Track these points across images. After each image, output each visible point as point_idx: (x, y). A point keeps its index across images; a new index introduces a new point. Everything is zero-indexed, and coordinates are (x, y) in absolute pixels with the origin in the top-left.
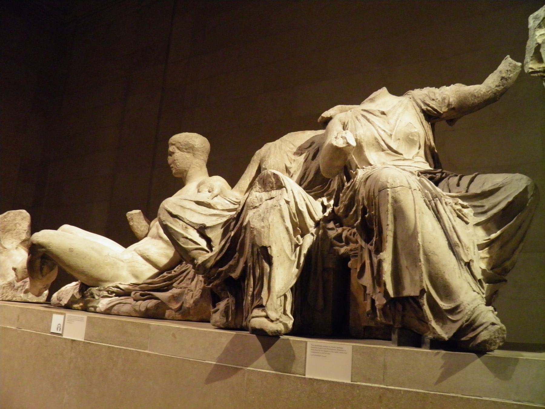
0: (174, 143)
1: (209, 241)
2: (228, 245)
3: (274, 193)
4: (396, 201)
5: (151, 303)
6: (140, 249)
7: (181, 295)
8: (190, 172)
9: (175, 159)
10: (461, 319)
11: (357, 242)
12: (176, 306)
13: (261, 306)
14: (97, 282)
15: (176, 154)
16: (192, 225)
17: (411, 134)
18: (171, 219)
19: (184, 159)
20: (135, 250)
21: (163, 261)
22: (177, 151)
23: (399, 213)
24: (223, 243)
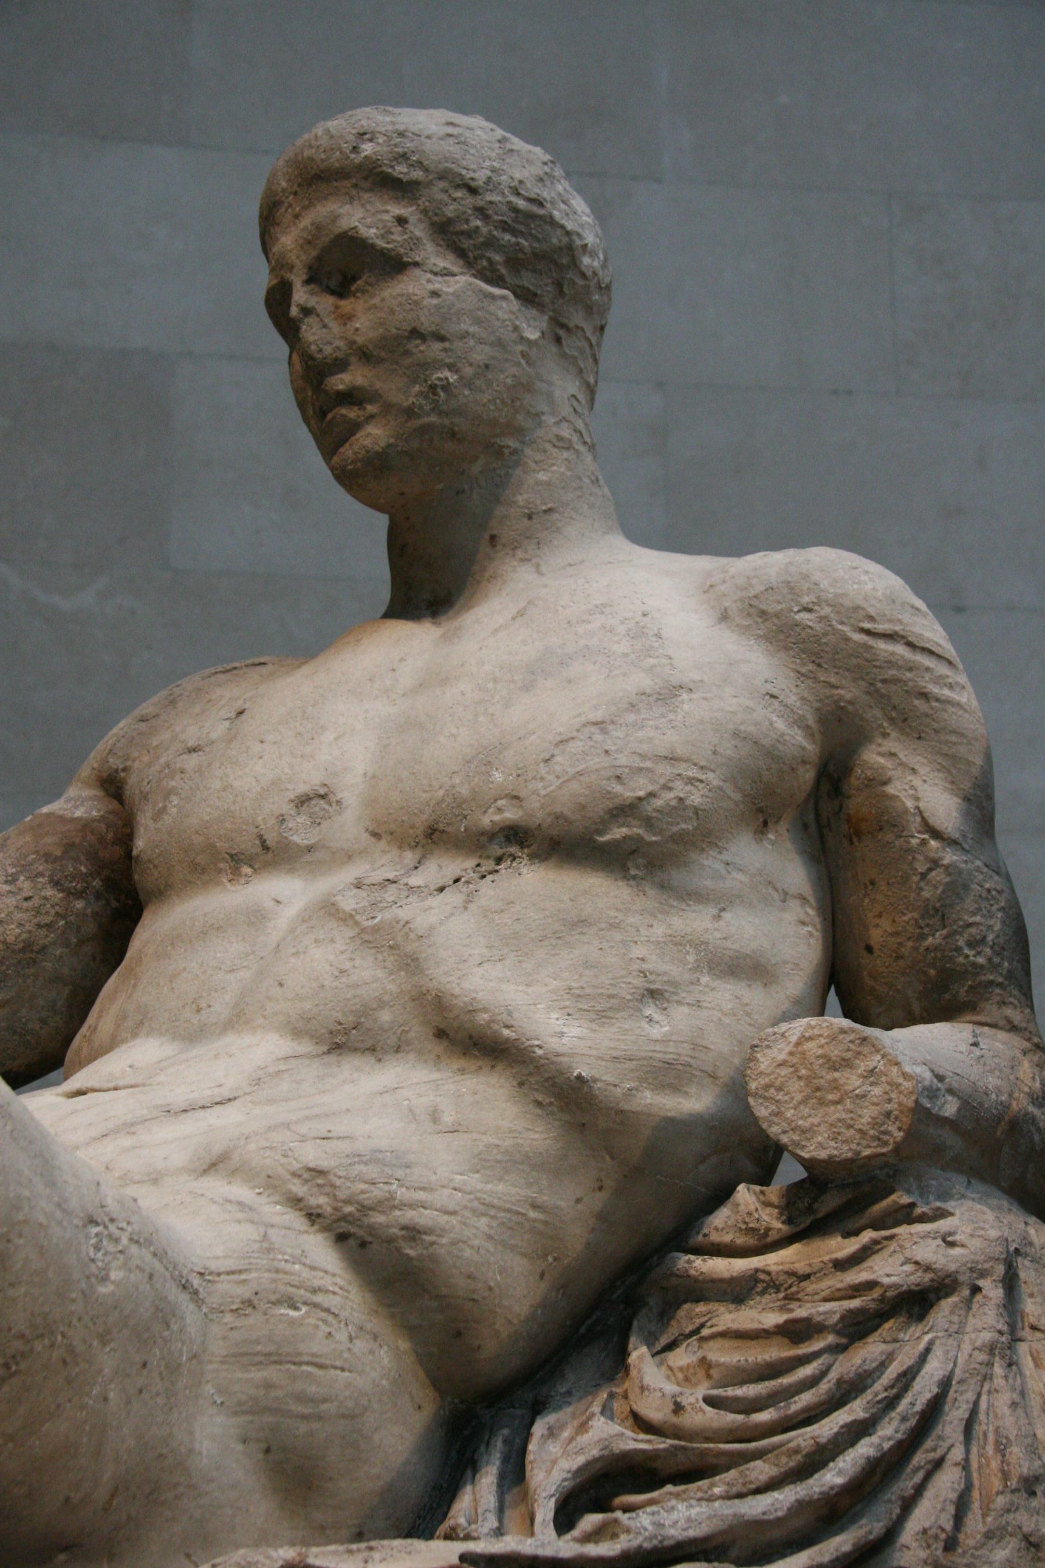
0: (400, 170)
6: (311, 1155)
8: (543, 473)
9: (427, 324)
15: (413, 285)
19: (500, 344)
20: (216, 1164)
22: (434, 255)
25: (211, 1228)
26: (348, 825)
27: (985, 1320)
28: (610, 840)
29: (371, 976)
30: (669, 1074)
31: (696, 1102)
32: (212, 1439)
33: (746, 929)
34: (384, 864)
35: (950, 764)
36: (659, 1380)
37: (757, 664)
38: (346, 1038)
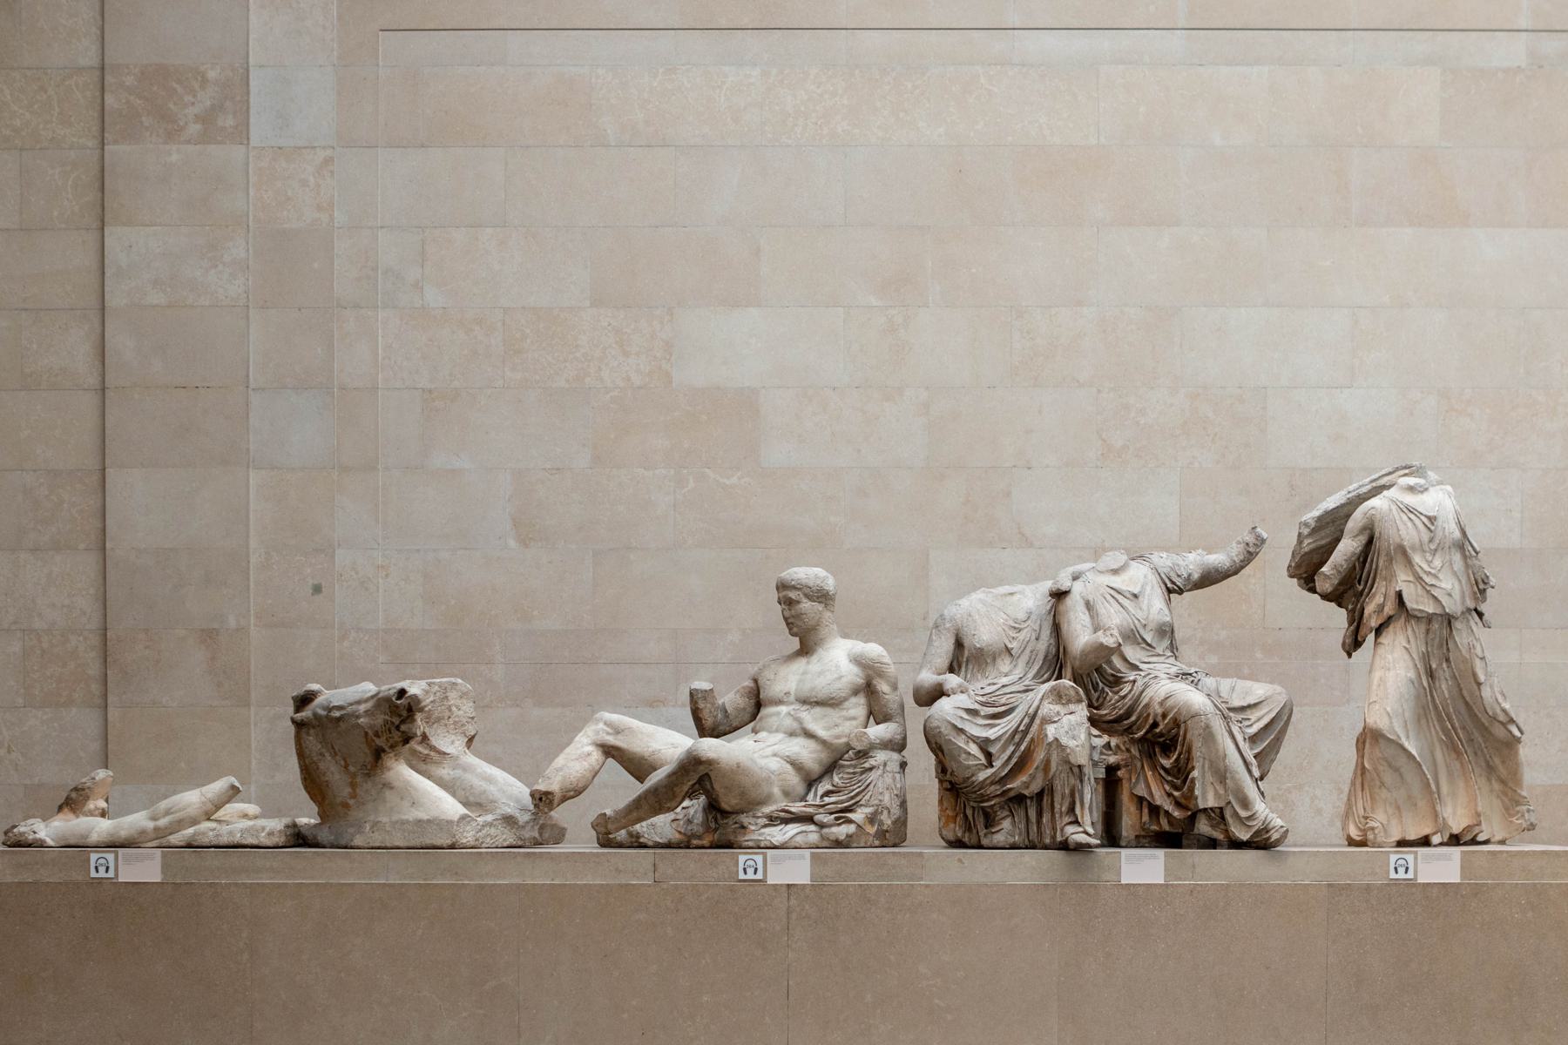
1: (989, 756)
2: (1014, 760)
3: (1072, 707)
4: (1208, 727)
5: (852, 828)
7: (875, 814)
8: (823, 632)
10: (1257, 824)
11: (1128, 750)
12: (872, 830)
13: (1076, 822)
14: (751, 804)
15: (802, 606)
16: (974, 739)
17: (1164, 624)
18: (953, 733)
20: (775, 755)
21: (814, 767)
23: (1208, 735)
24: (1005, 756)
25: (775, 764)
26: (792, 698)
27: (880, 772)
28: (829, 702)
29: (795, 725)
30: (838, 737)
31: (844, 740)
32: (776, 791)
33: (852, 712)
34: (797, 706)
35: (888, 682)
36: (836, 779)
37: (855, 669)
38: (792, 734)
